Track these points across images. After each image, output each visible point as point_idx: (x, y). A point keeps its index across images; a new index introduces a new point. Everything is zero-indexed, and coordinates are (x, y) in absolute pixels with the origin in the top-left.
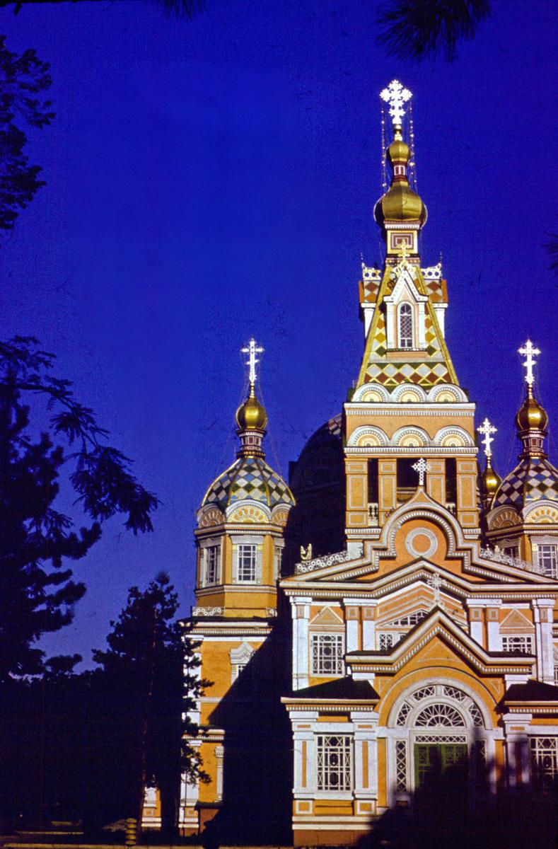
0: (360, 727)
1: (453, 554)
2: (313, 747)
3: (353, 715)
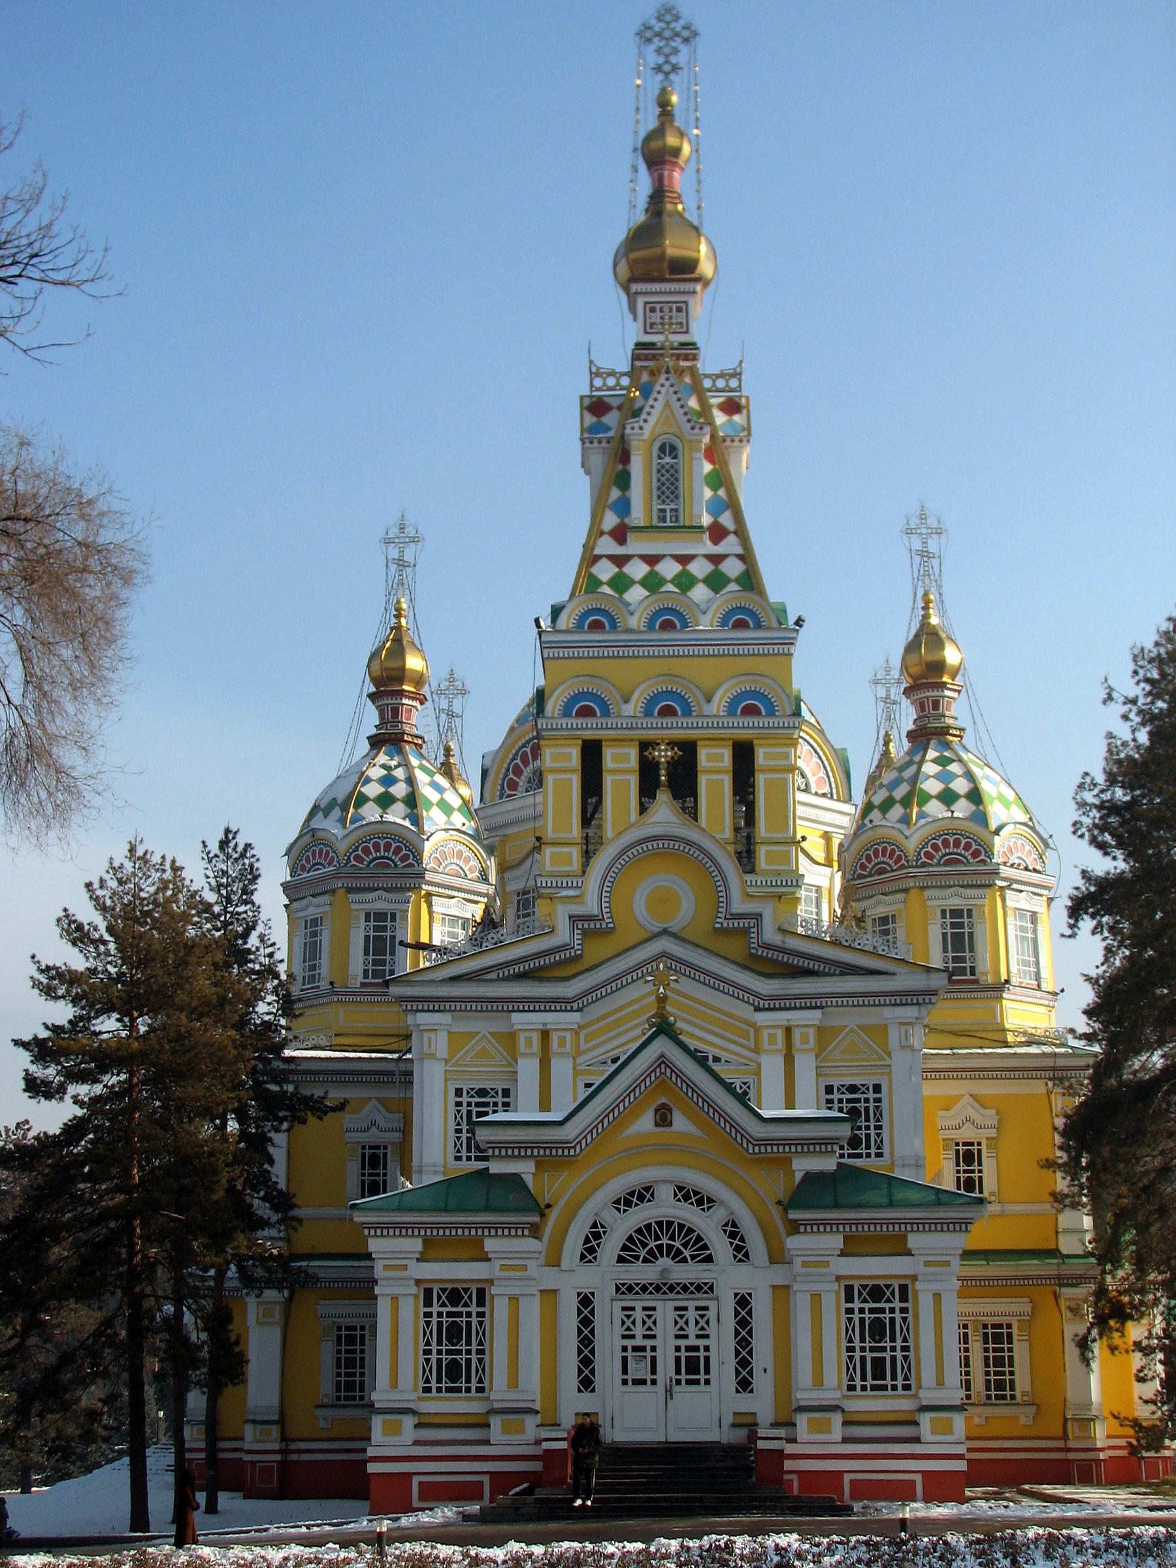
0: (504, 1267)
2: (410, 1312)
3: (490, 1245)
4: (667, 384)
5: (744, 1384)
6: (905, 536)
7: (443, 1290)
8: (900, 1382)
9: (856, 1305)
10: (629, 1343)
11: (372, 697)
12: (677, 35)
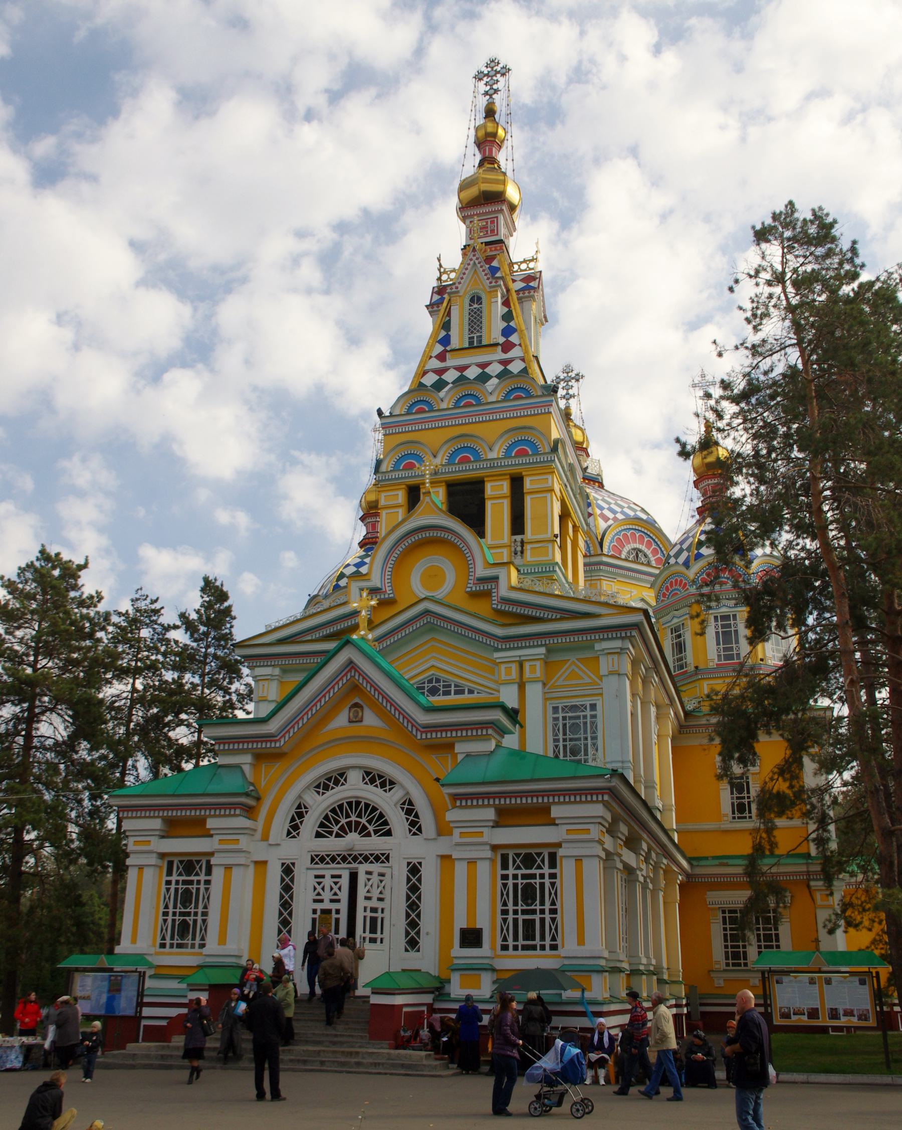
1: (474, 589)
3: (211, 823)
4: (474, 258)
5: (413, 944)
6: (692, 389)
7: (181, 862)
8: (548, 942)
9: (511, 871)
10: (319, 906)
11: (362, 519)
12: (499, 72)
